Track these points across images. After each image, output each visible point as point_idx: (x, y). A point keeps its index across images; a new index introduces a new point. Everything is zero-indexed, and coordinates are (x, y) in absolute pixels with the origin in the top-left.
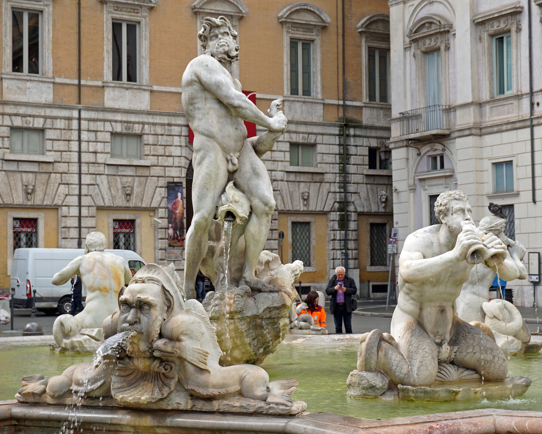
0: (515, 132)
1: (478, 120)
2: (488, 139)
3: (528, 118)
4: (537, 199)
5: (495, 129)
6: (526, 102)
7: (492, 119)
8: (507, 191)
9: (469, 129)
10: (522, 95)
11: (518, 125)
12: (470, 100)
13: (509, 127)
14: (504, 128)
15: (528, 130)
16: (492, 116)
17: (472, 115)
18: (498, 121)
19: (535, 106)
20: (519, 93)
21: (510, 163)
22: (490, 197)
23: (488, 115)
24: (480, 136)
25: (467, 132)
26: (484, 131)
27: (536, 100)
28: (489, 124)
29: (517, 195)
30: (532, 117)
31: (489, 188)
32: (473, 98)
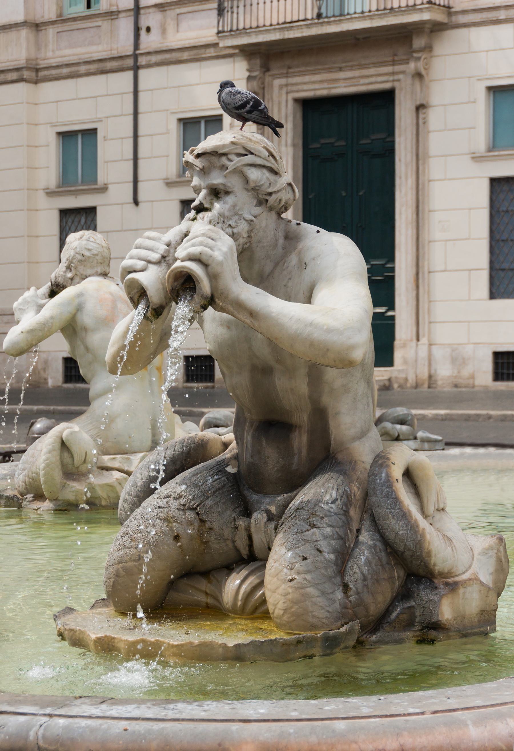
0: (103, 77)
1: (33, 56)
2: (49, 90)
3: (131, 53)
4: (141, 197)
5: (65, 71)
6: (125, 26)
7: (58, 53)
8: (83, 183)
9: (18, 69)
10: (119, 12)
11: (109, 65)
12: (20, 18)
13: (93, 67)
14: (83, 69)
15: (130, 74)
16: (59, 49)
17: (24, 45)
18: (71, 58)
19: (143, 33)
20: (114, 9)
21: (94, 132)
22: (50, 194)
23: (51, 47)
24: (36, 82)
25: (14, 76)
26: (41, 74)
27: (144, 23)
28: (53, 62)
29: (104, 189)
30: (138, 52)
31: (49, 174)
32: (26, 13)
